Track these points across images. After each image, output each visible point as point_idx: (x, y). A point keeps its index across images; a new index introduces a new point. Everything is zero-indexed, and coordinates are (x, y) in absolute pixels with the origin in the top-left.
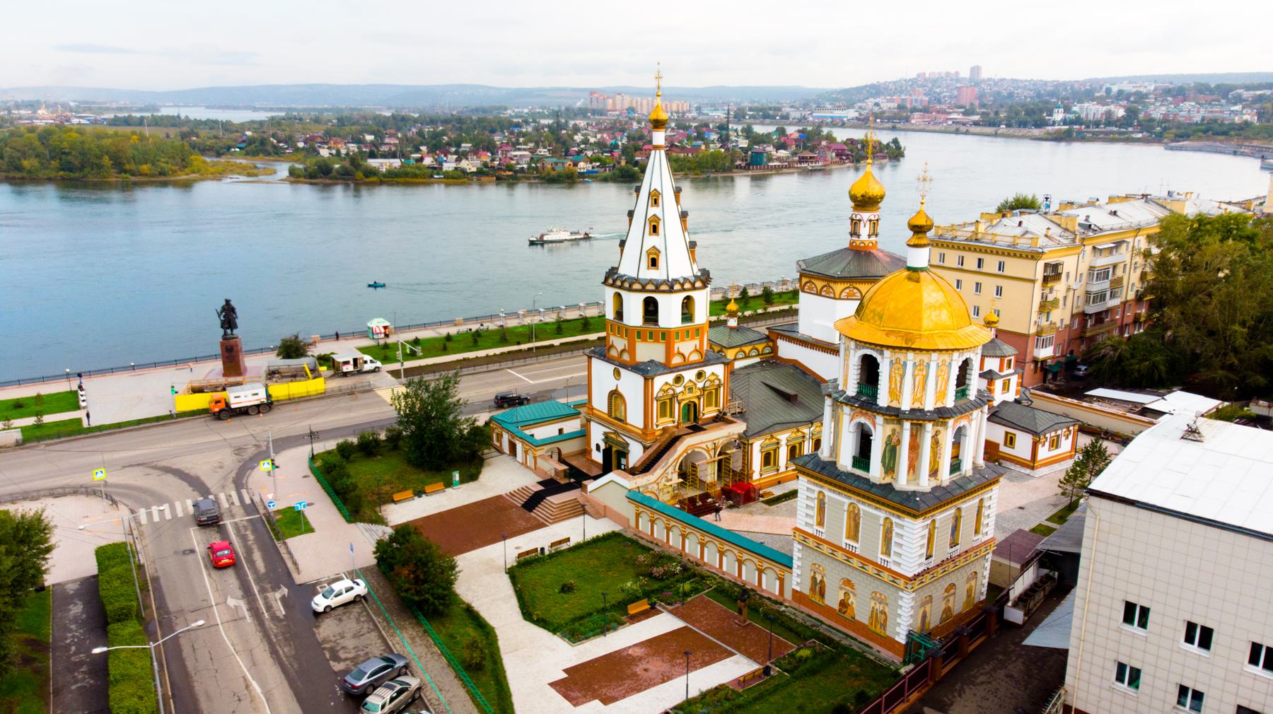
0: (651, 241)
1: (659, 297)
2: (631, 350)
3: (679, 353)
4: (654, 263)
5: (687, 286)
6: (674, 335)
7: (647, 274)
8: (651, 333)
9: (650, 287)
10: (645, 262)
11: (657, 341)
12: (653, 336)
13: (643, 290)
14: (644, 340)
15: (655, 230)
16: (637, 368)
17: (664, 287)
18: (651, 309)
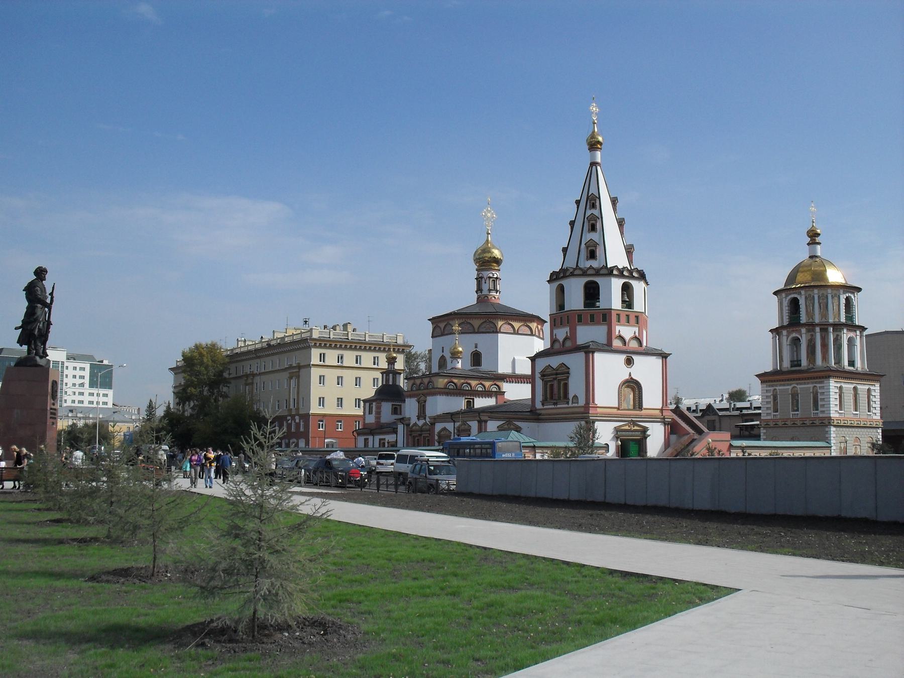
0: (589, 236)
1: (597, 279)
2: (572, 336)
3: (621, 338)
4: (592, 255)
5: (625, 273)
6: (614, 318)
7: (586, 264)
8: (592, 317)
9: (589, 272)
10: (584, 253)
11: (598, 323)
12: (593, 320)
13: (584, 273)
14: (586, 324)
15: (593, 228)
16: (577, 349)
17: (603, 271)
18: (592, 293)
